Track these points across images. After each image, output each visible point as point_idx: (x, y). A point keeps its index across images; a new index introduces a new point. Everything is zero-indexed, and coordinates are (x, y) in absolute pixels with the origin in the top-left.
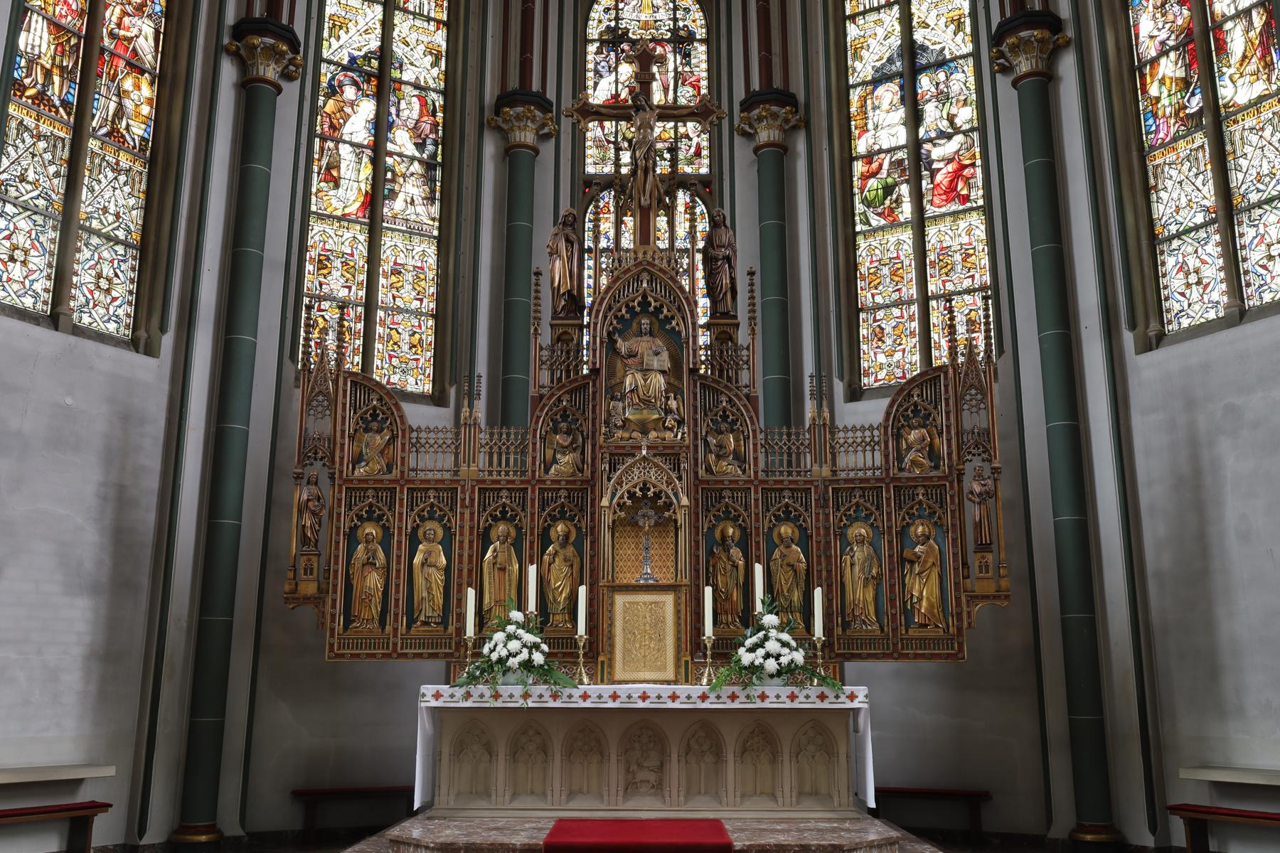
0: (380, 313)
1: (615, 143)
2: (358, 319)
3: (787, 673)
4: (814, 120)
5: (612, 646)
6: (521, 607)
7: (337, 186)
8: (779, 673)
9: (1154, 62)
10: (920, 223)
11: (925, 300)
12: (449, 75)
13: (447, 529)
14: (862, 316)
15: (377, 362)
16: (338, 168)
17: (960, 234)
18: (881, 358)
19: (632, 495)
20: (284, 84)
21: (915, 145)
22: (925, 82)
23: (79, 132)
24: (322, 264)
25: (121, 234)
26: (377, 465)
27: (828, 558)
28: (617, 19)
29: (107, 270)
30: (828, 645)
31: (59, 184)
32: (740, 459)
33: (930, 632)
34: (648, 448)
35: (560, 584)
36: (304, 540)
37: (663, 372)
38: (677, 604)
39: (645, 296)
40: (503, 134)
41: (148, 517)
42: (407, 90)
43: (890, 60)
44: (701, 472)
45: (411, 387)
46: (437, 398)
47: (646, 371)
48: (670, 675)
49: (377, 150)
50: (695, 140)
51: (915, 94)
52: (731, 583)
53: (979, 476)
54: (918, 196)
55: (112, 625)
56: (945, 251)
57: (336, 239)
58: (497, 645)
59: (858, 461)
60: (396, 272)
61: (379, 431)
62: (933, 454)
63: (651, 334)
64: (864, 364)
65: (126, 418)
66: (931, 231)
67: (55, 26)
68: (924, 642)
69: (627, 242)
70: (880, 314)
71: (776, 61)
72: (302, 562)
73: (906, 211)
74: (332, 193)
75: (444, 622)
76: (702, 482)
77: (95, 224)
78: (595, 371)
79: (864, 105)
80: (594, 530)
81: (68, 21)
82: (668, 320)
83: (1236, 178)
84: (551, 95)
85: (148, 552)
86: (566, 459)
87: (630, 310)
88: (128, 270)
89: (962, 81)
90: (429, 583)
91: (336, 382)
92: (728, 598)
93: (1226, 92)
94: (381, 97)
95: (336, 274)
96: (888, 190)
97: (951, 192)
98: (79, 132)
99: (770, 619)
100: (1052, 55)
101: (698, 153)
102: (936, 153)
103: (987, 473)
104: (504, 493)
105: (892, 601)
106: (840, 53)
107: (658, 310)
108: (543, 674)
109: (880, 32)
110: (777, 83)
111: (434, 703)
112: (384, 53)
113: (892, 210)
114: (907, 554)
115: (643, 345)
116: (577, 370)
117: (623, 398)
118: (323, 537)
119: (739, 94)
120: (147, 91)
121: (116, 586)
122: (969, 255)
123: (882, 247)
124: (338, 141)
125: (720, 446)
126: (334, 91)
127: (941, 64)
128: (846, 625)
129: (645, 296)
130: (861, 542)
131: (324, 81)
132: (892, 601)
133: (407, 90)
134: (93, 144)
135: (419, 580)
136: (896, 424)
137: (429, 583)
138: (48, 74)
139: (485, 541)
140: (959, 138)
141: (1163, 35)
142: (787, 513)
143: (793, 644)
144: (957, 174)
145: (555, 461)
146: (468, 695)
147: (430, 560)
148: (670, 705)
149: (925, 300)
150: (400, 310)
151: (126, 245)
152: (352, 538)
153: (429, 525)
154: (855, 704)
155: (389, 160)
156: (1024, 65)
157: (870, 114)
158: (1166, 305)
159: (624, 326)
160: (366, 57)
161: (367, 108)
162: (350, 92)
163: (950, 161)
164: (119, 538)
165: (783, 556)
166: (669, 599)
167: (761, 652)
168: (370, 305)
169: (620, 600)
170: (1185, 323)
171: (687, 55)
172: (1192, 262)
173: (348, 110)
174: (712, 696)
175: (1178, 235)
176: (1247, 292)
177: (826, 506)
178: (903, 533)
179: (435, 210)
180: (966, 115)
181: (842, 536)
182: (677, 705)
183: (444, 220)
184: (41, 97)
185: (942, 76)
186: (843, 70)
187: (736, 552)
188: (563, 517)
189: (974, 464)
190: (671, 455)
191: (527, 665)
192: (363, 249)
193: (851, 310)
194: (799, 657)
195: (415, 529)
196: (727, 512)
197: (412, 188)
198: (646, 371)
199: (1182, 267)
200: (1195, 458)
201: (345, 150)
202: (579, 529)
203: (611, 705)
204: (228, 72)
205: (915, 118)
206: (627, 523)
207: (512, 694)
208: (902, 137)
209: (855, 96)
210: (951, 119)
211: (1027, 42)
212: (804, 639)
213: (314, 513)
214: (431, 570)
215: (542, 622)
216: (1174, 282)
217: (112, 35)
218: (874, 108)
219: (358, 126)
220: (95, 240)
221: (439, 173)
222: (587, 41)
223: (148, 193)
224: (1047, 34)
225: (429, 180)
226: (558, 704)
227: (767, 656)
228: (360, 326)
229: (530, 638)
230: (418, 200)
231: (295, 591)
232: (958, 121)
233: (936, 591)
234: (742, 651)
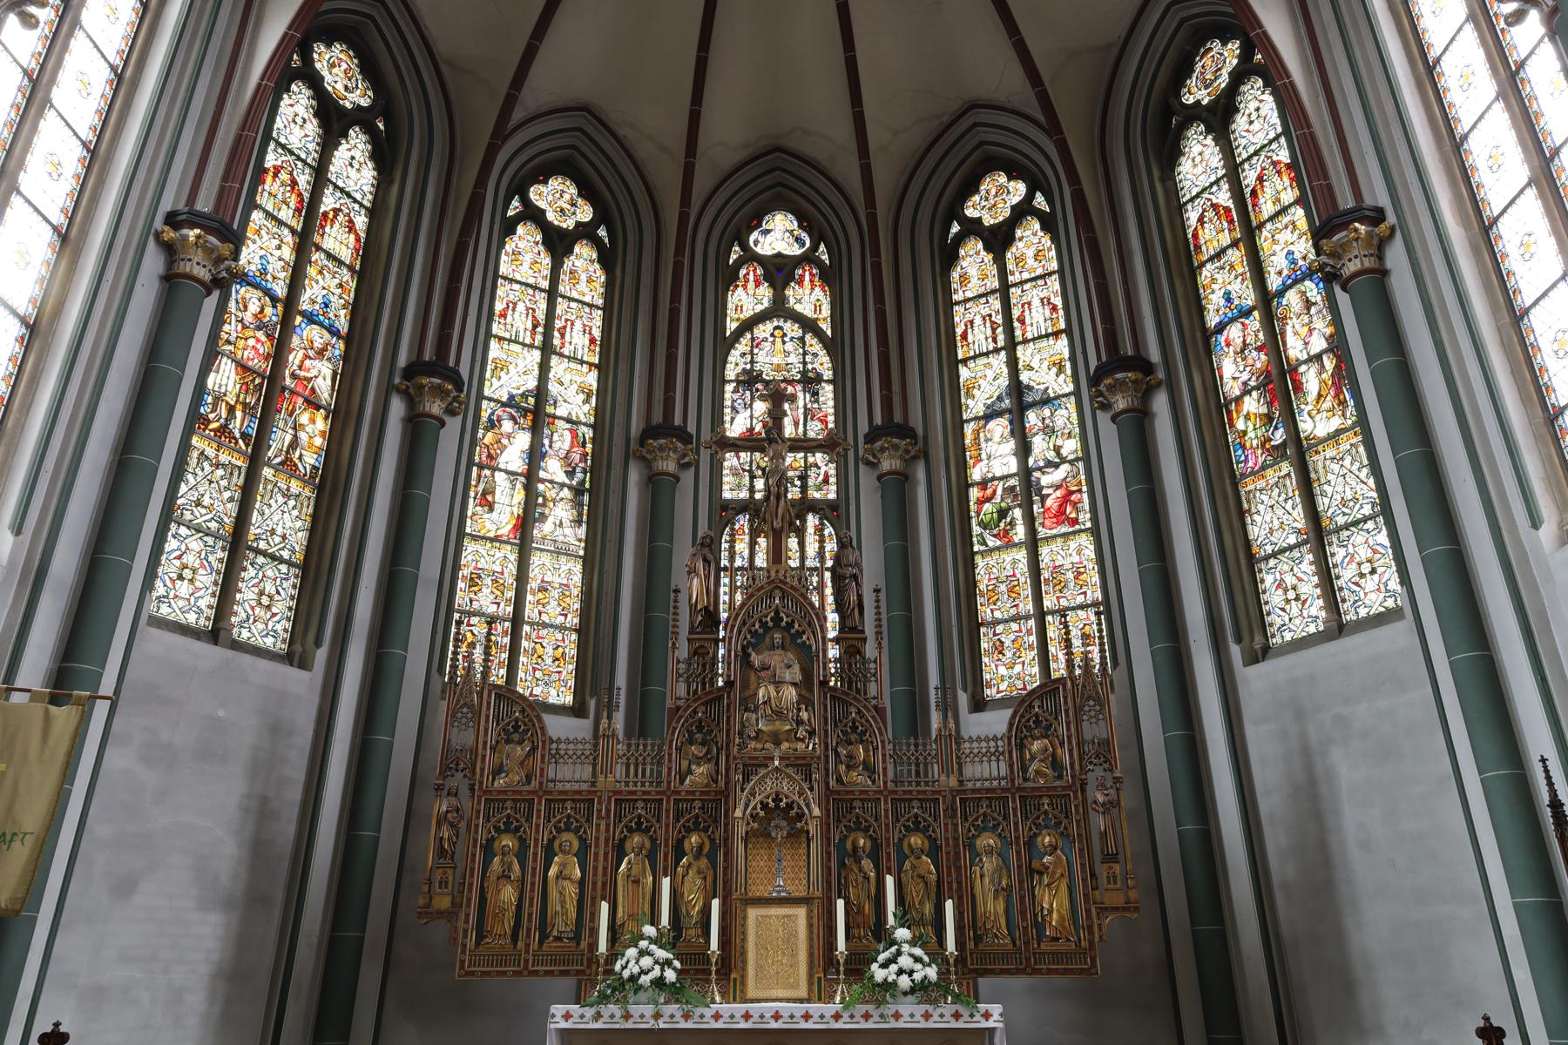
0: (526, 628)
1: (750, 471)
2: (505, 633)
3: (921, 990)
4: (932, 451)
5: (745, 962)
6: (654, 921)
7: (491, 510)
8: (913, 991)
9: (1238, 400)
10: (1033, 544)
11: (1041, 615)
12: (598, 411)
13: (583, 840)
14: (983, 630)
15: (521, 674)
16: (493, 493)
17: (1071, 553)
18: (1002, 670)
19: (764, 806)
20: (447, 419)
21: (1026, 473)
22: (1032, 418)
23: (255, 461)
24: (473, 582)
25: (286, 554)
27: (958, 868)
28: (752, 362)
29: (269, 588)
30: (960, 960)
31: (233, 508)
32: (869, 769)
33: (1061, 946)
34: (781, 758)
35: (693, 896)
36: (441, 853)
37: (795, 684)
38: (809, 918)
39: (777, 612)
40: (647, 463)
41: (287, 828)
42: (561, 424)
43: (1000, 398)
44: (832, 783)
45: (553, 699)
46: (577, 710)
47: (778, 684)
48: (803, 993)
49: (530, 478)
50: (824, 469)
51: (1024, 428)
52: (863, 896)
53: (1102, 786)
54: (1030, 520)
55: (242, 941)
57: (486, 559)
58: (630, 962)
59: (984, 772)
60: (543, 589)
61: (520, 742)
62: (1056, 764)
63: (783, 647)
64: (987, 676)
65: (276, 730)
66: (1044, 551)
67: (242, 367)
68: (1057, 956)
69: (761, 561)
70: (999, 629)
71: (897, 400)
72: (438, 875)
73: (1020, 532)
74: (486, 516)
75: (577, 938)
76: (833, 792)
77: (262, 545)
78: (729, 684)
79: (977, 438)
80: (727, 841)
81: (256, 363)
82: (800, 634)
83: (1322, 503)
84: (692, 428)
85: (286, 864)
86: (700, 770)
87: (763, 625)
88: (289, 588)
89: (1066, 416)
90: (563, 898)
91: (480, 694)
92: (860, 911)
93: (1305, 426)
94: (536, 430)
95: (486, 591)
96: (1002, 513)
97: (1060, 516)
98: (255, 461)
99: (903, 933)
100: (1147, 394)
101: (826, 481)
102: (1045, 480)
103: (1109, 783)
104: (640, 804)
105: (1023, 913)
106: (954, 392)
107: (790, 625)
108: (675, 992)
109: (990, 374)
110: (898, 418)
111: (563, 1025)
112: (541, 393)
113: (1006, 532)
114: (1035, 864)
115: (776, 659)
116: (713, 681)
117: (756, 710)
118: (460, 848)
120: (321, 425)
121: (251, 901)
122: (1080, 574)
123: (1000, 566)
124: (494, 469)
125: (850, 757)
126: (492, 424)
127: (1046, 401)
128: (978, 939)
129: (777, 612)
130: (990, 853)
131: (485, 415)
132: (1023, 913)
133: (561, 424)
134: (267, 472)
135: (553, 894)
136: (1019, 734)
137: (563, 898)
138: (231, 410)
139: (620, 853)
140: (1065, 467)
141: (1245, 376)
142: (917, 823)
143: (926, 959)
144: (1065, 499)
145: (690, 772)
146: (598, 1016)
147: (565, 873)
148: (804, 1025)
149: (1041, 615)
150: (545, 625)
151: (290, 563)
152: (488, 851)
153: (565, 836)
154: (990, 1024)
155: (541, 487)
156: (1121, 403)
157: (983, 445)
158: (1268, 619)
159: (757, 640)
160: (524, 396)
161: (523, 440)
162: (507, 426)
163: (1058, 487)
164: (257, 850)
165: (914, 867)
166: (801, 912)
167: (894, 968)
168: (517, 620)
169: (753, 913)
170: (1288, 636)
171: (815, 394)
172: (1290, 580)
173: (505, 441)
174: (846, 1015)
175: (1274, 555)
176: (1344, 607)
177: (954, 816)
178: (1030, 843)
179: (582, 532)
180: (1070, 447)
181: (971, 846)
182: (810, 1025)
183: (589, 541)
184: (223, 430)
185: (1047, 412)
186: (958, 407)
187: (867, 864)
188: (697, 828)
189: (1096, 774)
190: (802, 766)
191: (659, 983)
192: (512, 568)
193: (972, 626)
194: (932, 973)
195: (551, 841)
196: (858, 823)
198: (778, 684)
199: (1280, 584)
200: (1309, 767)
201: (500, 478)
202: (712, 841)
203: (743, 1025)
204: (397, 408)
205: (1024, 449)
206: (759, 835)
207: (643, 1014)
208: (1013, 468)
209: (969, 429)
210: (1057, 449)
211: (1123, 382)
212: (936, 952)
213: (452, 825)
214: (566, 883)
215: (674, 938)
216: (1274, 598)
217: (293, 376)
218: (987, 440)
219: (514, 456)
220: (261, 560)
221: (586, 498)
222: (725, 382)
223: (314, 516)
224: (1140, 376)
225: (578, 505)
226: (689, 1025)
227: (900, 972)
228: (507, 640)
229: (662, 954)
230: (566, 523)
231: (429, 905)
232: (1064, 452)
233: (1066, 902)
234: (874, 966)
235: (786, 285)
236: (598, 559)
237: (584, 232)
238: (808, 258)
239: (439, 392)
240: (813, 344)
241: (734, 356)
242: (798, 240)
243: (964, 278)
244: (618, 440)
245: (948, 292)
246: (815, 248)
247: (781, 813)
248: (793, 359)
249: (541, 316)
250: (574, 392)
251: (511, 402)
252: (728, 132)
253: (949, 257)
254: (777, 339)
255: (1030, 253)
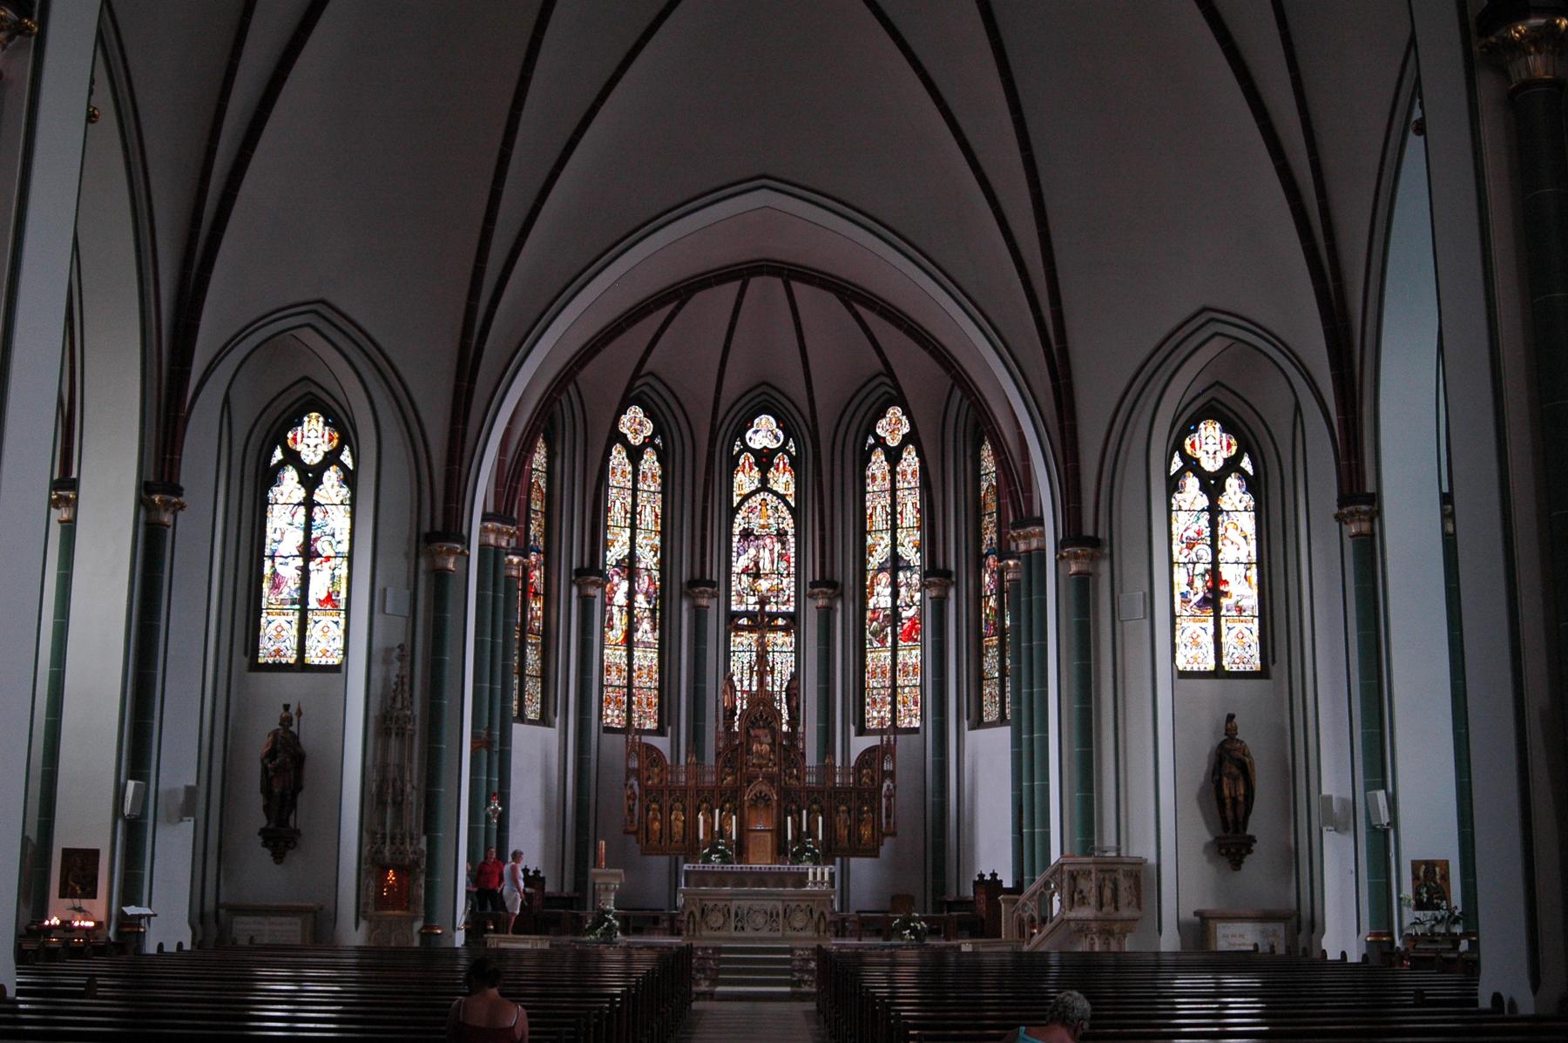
12: (662, 562)
17: (911, 656)
21: (895, 607)
22: (901, 575)
26: (656, 781)
32: (798, 778)
56: (905, 665)
57: (615, 655)
62: (872, 779)
65: (546, 756)
69: (754, 688)
73: (889, 644)
90: (678, 826)
102: (904, 614)
106: (863, 552)
115: (760, 732)
119: (810, 579)
123: (878, 657)
144: (912, 627)
159: (753, 725)
161: (625, 586)
162: (616, 579)
164: (547, 803)
183: (661, 640)
186: (864, 562)
190: (770, 779)
192: (625, 660)
197: (646, 625)
201: (615, 610)
204: (575, 590)
206: (754, 805)
219: (620, 598)
225: (653, 617)
235: (768, 470)
236: (665, 649)
237: (649, 442)
238: (783, 449)
239: (594, 583)
240: (786, 514)
241: (739, 519)
242: (776, 437)
243: (874, 478)
244: (676, 586)
245: (863, 485)
246: (786, 443)
247: (761, 799)
248: (771, 521)
249: (629, 508)
250: (648, 559)
251: (619, 563)
252: (733, 386)
253: (866, 460)
254: (763, 558)
255: (909, 471)
